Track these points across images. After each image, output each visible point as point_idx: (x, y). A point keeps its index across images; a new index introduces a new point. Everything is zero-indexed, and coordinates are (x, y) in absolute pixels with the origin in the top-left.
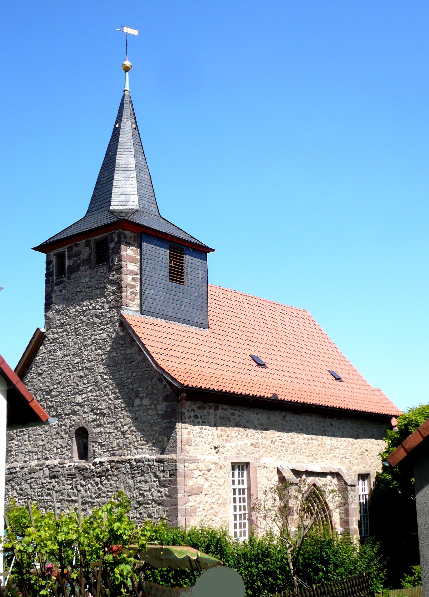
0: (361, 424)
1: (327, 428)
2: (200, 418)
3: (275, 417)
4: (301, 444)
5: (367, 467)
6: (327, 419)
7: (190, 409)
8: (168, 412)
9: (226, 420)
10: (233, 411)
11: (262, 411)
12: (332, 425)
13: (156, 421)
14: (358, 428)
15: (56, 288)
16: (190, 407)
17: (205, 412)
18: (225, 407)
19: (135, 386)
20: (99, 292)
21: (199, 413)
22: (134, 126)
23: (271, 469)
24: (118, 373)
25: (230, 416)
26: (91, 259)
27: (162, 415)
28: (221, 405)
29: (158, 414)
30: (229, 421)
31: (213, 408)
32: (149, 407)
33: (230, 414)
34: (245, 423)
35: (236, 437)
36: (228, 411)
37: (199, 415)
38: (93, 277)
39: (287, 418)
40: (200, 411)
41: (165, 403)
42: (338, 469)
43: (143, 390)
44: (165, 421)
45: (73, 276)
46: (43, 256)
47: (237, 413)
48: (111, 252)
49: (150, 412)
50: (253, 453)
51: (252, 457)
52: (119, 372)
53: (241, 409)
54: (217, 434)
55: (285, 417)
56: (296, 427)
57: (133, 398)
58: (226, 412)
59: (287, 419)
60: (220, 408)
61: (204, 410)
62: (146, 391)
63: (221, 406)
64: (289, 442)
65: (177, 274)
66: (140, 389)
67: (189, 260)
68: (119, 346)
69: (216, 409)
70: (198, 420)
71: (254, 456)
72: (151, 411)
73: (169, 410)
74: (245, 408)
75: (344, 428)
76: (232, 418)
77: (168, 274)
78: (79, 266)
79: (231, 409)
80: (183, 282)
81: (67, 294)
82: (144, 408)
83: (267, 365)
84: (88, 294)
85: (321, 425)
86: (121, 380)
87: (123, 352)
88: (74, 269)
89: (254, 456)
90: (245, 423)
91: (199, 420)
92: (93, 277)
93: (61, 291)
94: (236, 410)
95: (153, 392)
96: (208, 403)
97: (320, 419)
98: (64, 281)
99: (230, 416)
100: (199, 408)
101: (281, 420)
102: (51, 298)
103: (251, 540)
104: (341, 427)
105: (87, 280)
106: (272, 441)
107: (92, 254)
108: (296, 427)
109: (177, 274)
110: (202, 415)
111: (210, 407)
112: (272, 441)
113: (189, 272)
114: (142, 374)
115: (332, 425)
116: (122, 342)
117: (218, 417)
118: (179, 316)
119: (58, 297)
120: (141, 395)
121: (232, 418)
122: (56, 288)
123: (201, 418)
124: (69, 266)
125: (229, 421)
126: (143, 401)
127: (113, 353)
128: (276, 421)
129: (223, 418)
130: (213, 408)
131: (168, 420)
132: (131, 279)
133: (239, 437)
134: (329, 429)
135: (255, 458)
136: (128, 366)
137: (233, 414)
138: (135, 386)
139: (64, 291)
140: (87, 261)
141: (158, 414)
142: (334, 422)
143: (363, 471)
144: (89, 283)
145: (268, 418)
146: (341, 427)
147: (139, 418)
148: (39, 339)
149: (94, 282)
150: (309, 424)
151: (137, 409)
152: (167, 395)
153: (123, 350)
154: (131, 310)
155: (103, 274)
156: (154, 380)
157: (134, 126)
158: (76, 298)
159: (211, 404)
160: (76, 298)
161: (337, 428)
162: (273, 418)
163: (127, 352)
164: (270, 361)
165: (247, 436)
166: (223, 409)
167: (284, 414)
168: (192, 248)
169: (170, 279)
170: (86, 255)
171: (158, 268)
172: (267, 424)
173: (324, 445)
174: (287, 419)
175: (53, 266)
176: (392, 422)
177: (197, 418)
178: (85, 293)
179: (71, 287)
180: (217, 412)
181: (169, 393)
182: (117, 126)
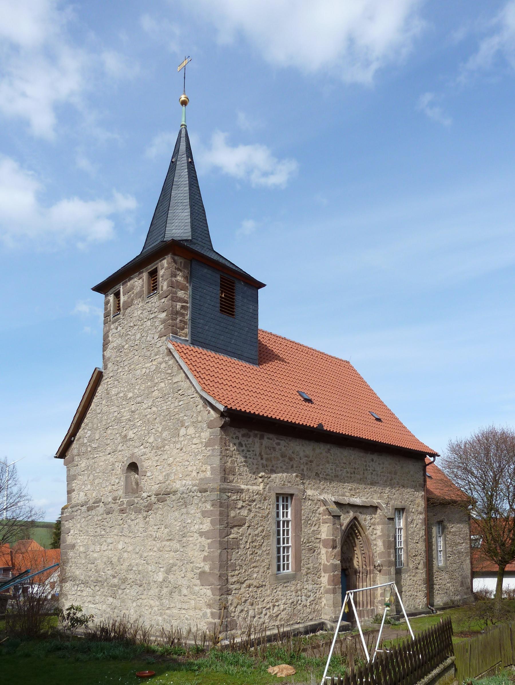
0: (399, 462)
1: (368, 464)
2: (244, 446)
3: (320, 448)
4: (344, 478)
5: (403, 502)
6: (369, 455)
7: (234, 436)
8: (212, 438)
9: (272, 450)
10: (278, 441)
11: (307, 442)
12: (373, 461)
13: (200, 450)
14: (396, 464)
15: (112, 326)
16: (235, 434)
17: (250, 440)
18: (271, 436)
19: (182, 415)
20: (149, 323)
21: (244, 441)
22: (190, 160)
23: (315, 502)
24: (166, 404)
25: (275, 446)
26: (143, 291)
27: (206, 443)
28: (266, 434)
29: (202, 443)
30: (275, 450)
31: (259, 436)
32: (193, 436)
33: (276, 443)
34: (291, 453)
35: (281, 467)
36: (274, 441)
37: (243, 443)
38: (145, 309)
39: (332, 451)
40: (244, 439)
41: (209, 430)
42: (378, 503)
43: (188, 418)
44: (208, 448)
45: (128, 311)
46: (101, 297)
47: (282, 442)
48: (161, 279)
49: (195, 441)
50: (298, 485)
51: (297, 488)
52: (166, 403)
53: (287, 439)
54: (262, 464)
55: (329, 450)
56: (340, 460)
57: (179, 428)
58: (271, 441)
59: (331, 452)
60: (265, 437)
61: (249, 438)
62: (191, 419)
63: (266, 435)
64: (333, 475)
65: (228, 307)
66: (185, 418)
67: (240, 286)
68: (168, 376)
69: (262, 437)
70: (243, 448)
71: (298, 487)
72: (195, 439)
73: (212, 437)
74: (291, 438)
75: (383, 463)
76: (277, 447)
77: (219, 305)
78: (132, 300)
79: (277, 439)
80: (233, 315)
81: (123, 331)
82: (189, 437)
83: (314, 401)
84: (140, 327)
85: (363, 460)
86: (168, 411)
87: (170, 382)
88: (129, 304)
89: (298, 487)
90: (291, 453)
91: (244, 448)
92: (145, 309)
93: (117, 329)
94: (282, 440)
95: (198, 420)
96: (253, 431)
97: (362, 454)
98: (118, 319)
99: (275, 446)
100: (243, 436)
101: (326, 452)
102: (108, 337)
103: (445, 537)
104: (381, 463)
105: (139, 312)
106: (317, 473)
107: (144, 285)
108: (340, 460)
109: (228, 307)
110: (247, 443)
111: (255, 436)
112: (317, 473)
113: (239, 305)
114: (187, 402)
115: (373, 461)
116: (169, 371)
117: (263, 446)
118: (229, 349)
119: (114, 335)
120: (186, 424)
121: (277, 447)
122: (112, 326)
123: (246, 446)
124: (124, 302)
125: (275, 450)
126: (188, 431)
127: (161, 384)
128: (321, 453)
129: (268, 448)
130: (259, 436)
131: (211, 448)
132: (180, 307)
133: (284, 467)
134: (370, 464)
135: (299, 489)
136: (175, 395)
137: (278, 444)
138: (182, 415)
139: (119, 328)
140: (140, 295)
141: (202, 443)
142: (375, 457)
143: (399, 505)
144: (141, 315)
145: (314, 450)
146: (381, 463)
147: (184, 449)
148: (98, 378)
149: (146, 314)
150: (352, 458)
151: (182, 439)
152: (211, 421)
153: (170, 379)
154: (180, 339)
155: (153, 304)
156: (199, 406)
157: (190, 160)
158: (129, 333)
159: (256, 432)
160: (129, 333)
161: (377, 464)
162: (318, 451)
163: (174, 381)
164: (316, 398)
165: (292, 467)
166: (268, 438)
167: (328, 446)
168: (244, 282)
169: (221, 310)
170: (139, 288)
171: (208, 298)
172: (313, 456)
173: (365, 480)
174: (331, 452)
175: (111, 305)
176: (426, 460)
177: (242, 446)
178: (137, 327)
179: (126, 323)
180: (262, 441)
181: (212, 419)
182: (173, 160)
